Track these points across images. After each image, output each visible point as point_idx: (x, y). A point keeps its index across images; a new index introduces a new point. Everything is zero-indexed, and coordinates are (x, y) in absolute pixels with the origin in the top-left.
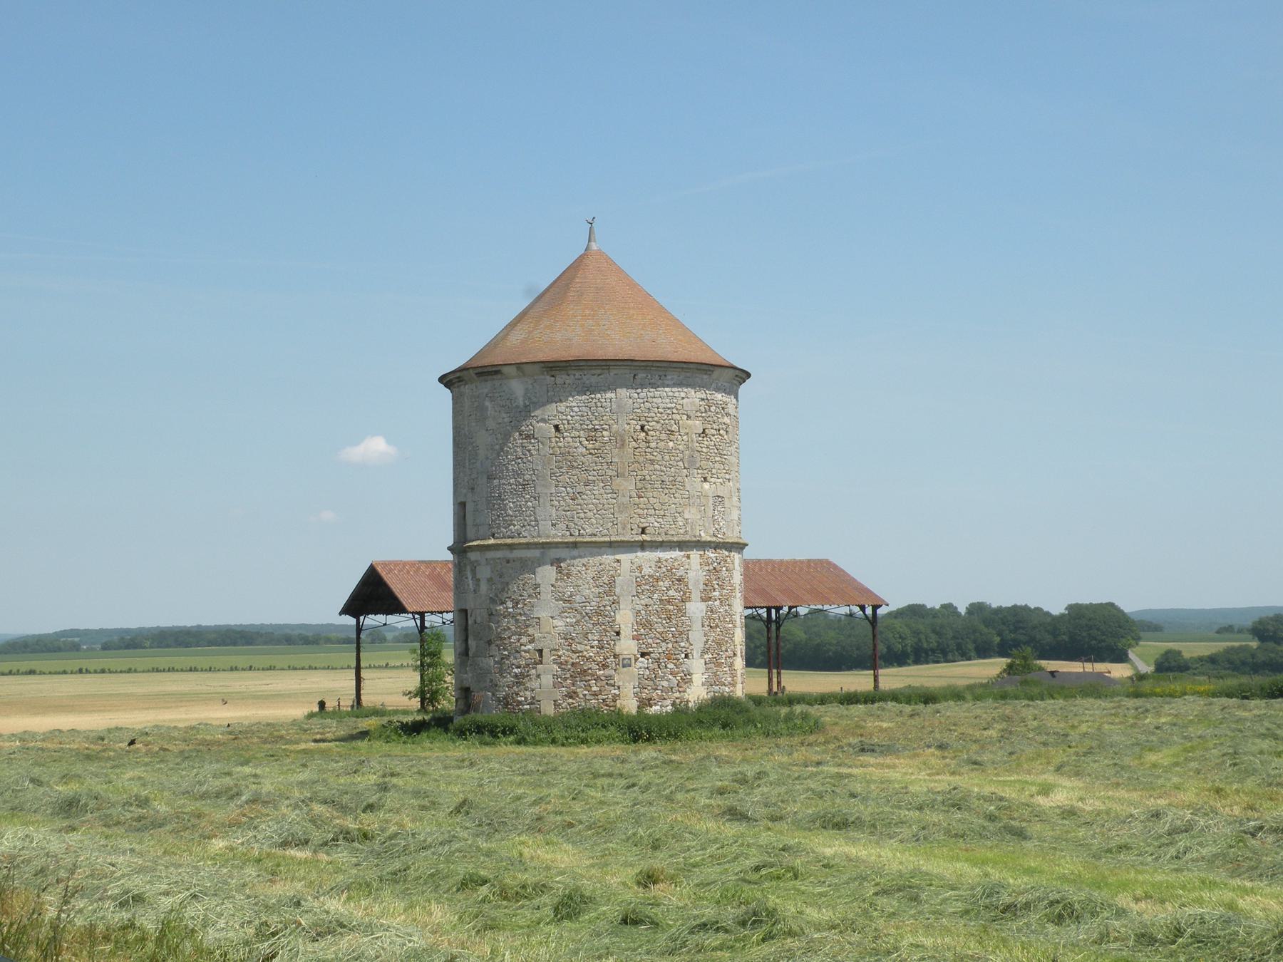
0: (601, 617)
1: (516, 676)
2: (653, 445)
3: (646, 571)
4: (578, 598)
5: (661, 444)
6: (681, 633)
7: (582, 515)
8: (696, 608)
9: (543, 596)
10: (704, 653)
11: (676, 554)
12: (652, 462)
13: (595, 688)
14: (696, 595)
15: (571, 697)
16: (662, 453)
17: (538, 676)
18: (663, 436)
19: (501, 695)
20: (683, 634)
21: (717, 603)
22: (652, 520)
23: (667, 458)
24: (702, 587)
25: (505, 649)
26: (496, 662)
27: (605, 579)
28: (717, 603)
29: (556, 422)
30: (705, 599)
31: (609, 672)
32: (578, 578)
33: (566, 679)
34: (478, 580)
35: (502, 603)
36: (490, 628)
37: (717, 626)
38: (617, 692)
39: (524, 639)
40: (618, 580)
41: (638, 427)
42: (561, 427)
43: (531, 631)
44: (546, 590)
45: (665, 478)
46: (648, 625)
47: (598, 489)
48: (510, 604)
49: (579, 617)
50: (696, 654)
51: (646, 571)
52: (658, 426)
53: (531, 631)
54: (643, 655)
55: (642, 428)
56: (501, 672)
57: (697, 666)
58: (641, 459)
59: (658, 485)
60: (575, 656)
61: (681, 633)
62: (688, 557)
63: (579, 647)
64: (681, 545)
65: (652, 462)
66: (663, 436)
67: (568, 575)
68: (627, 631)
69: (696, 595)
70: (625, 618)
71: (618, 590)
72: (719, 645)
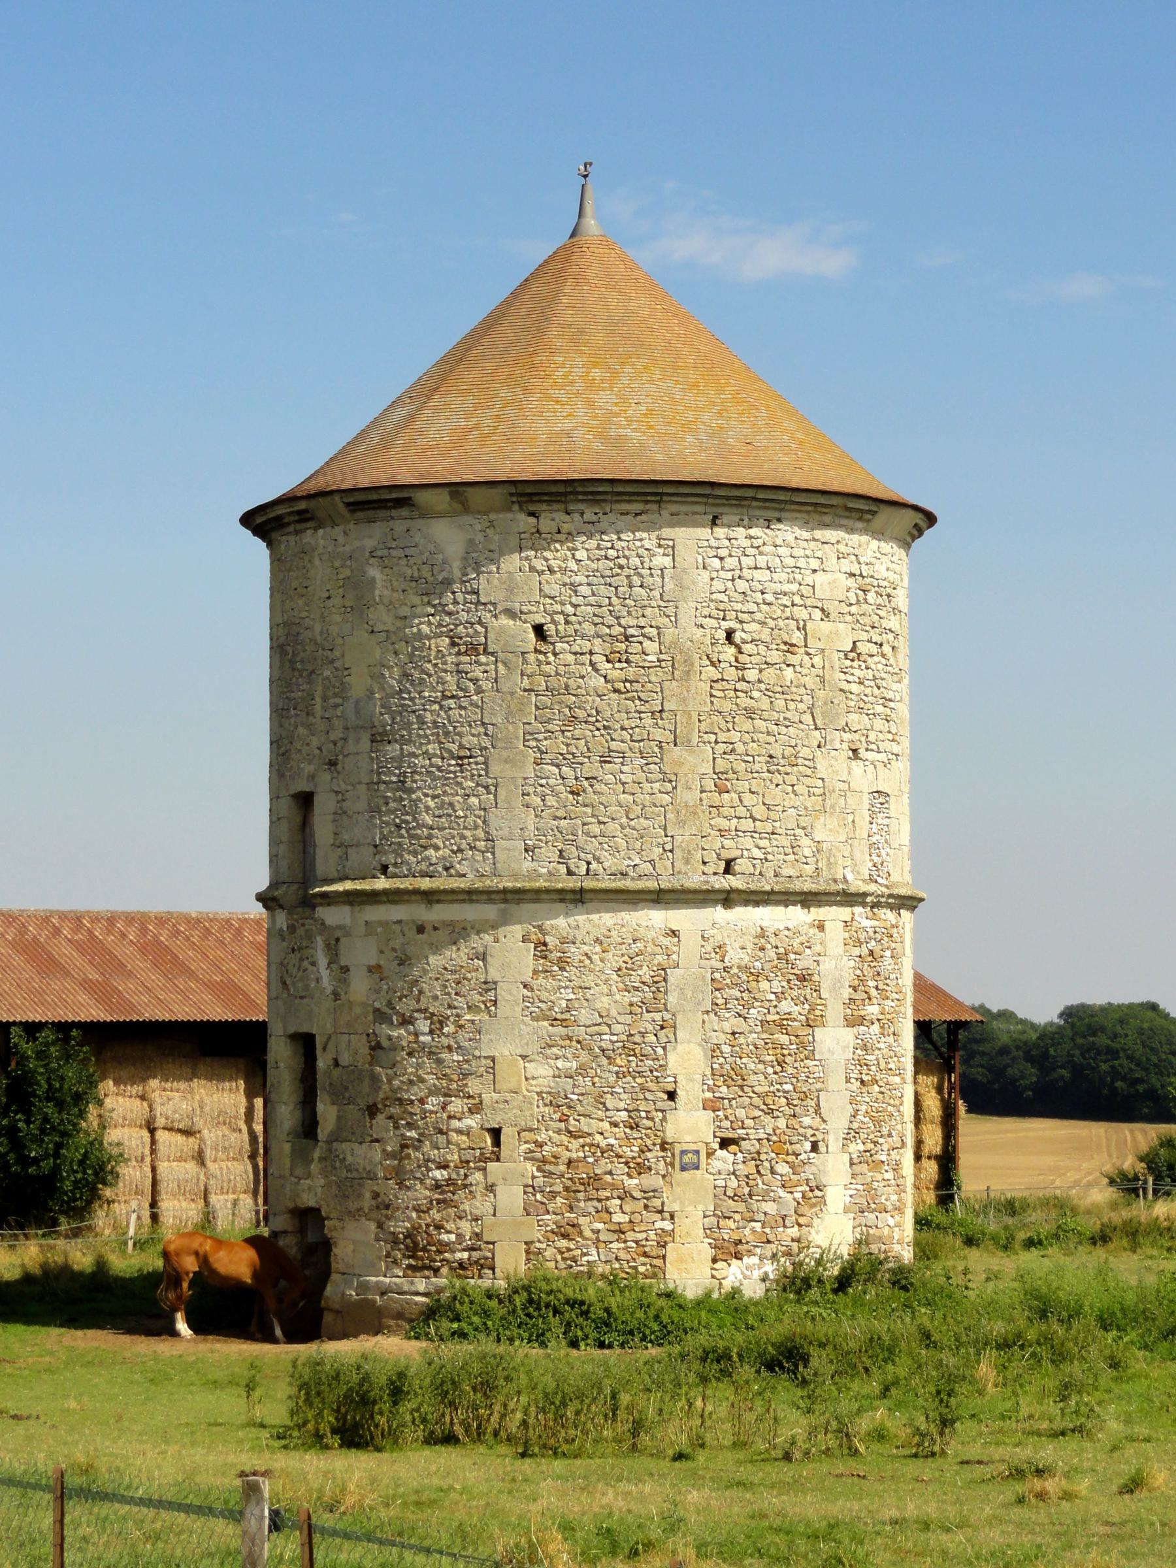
0: (636, 1055)
1: (437, 1186)
2: (751, 675)
3: (735, 956)
4: (584, 1015)
5: (770, 674)
6: (805, 1096)
7: (596, 829)
8: (835, 1041)
9: (503, 1009)
10: (851, 1135)
11: (795, 916)
12: (750, 714)
13: (618, 1218)
14: (835, 1011)
15: (565, 1236)
16: (768, 692)
17: (491, 1188)
18: (775, 656)
19: (400, 1227)
20: (806, 1098)
21: (875, 1028)
22: (747, 842)
23: (780, 704)
24: (847, 993)
25: (410, 1126)
26: (388, 1155)
27: (645, 973)
28: (875, 1028)
29: (539, 619)
30: (854, 1021)
31: (651, 1181)
32: (581, 967)
33: (554, 1195)
34: (345, 970)
35: (406, 1021)
36: (375, 1079)
37: (875, 1081)
38: (667, 1225)
39: (457, 1105)
40: (674, 976)
41: (721, 635)
42: (550, 629)
43: (473, 1086)
44: (510, 995)
45: (777, 750)
46: (736, 1078)
47: (631, 771)
48: (423, 1026)
49: (584, 1057)
50: (834, 1142)
51: (735, 956)
52: (765, 635)
53: (473, 1086)
54: (725, 1143)
55: (729, 635)
56: (400, 1176)
57: (834, 1169)
58: (727, 706)
59: (761, 765)
60: (576, 1144)
61: (805, 1096)
62: (821, 927)
63: (585, 1125)
64: (808, 899)
65: (750, 714)
66: (775, 656)
67: (563, 963)
68: (691, 1092)
69: (835, 1011)
70: (687, 1062)
71: (672, 999)
72: (878, 1123)
